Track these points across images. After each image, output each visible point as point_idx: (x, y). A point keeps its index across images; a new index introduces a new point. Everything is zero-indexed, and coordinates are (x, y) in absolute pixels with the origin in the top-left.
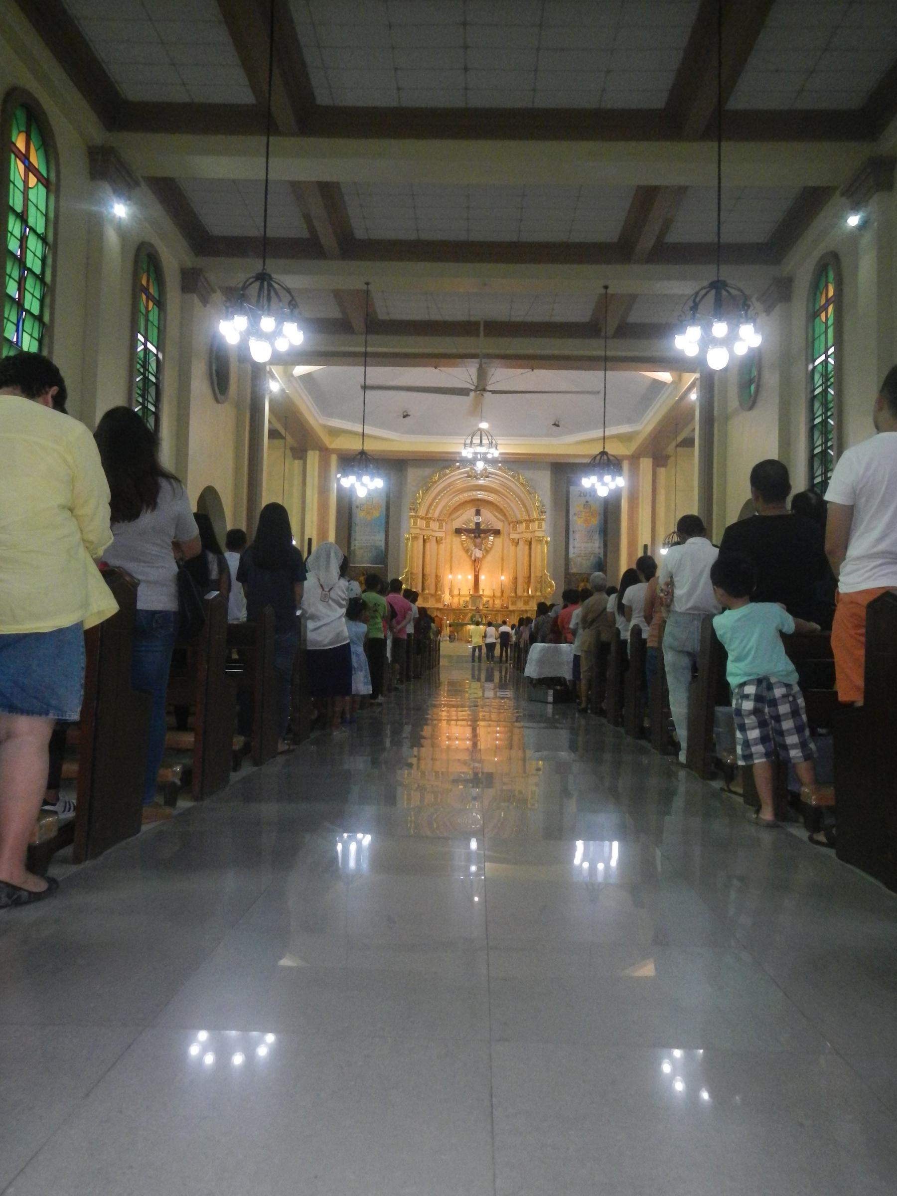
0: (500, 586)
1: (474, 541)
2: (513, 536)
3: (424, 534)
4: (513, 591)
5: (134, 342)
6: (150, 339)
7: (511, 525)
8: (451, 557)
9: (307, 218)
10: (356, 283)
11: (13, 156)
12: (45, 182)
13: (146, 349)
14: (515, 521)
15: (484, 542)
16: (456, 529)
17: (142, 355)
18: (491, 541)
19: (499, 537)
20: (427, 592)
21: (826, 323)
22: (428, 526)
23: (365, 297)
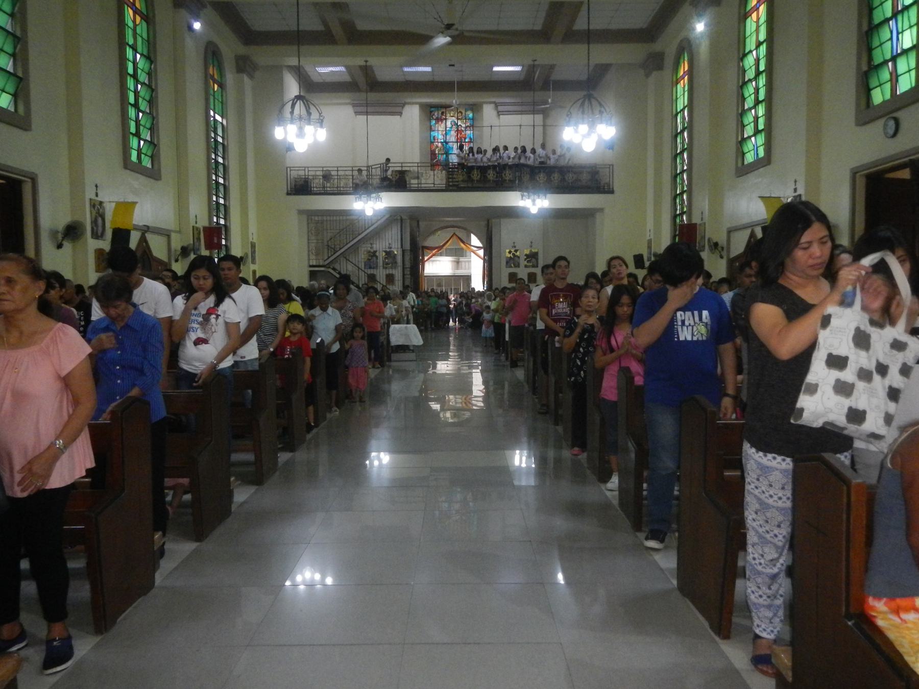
5: (207, 115)
6: (216, 111)
9: (324, 23)
10: (360, 62)
11: (126, 6)
12: (146, 18)
13: (215, 120)
17: (212, 123)
21: (684, 88)
23: (366, 70)
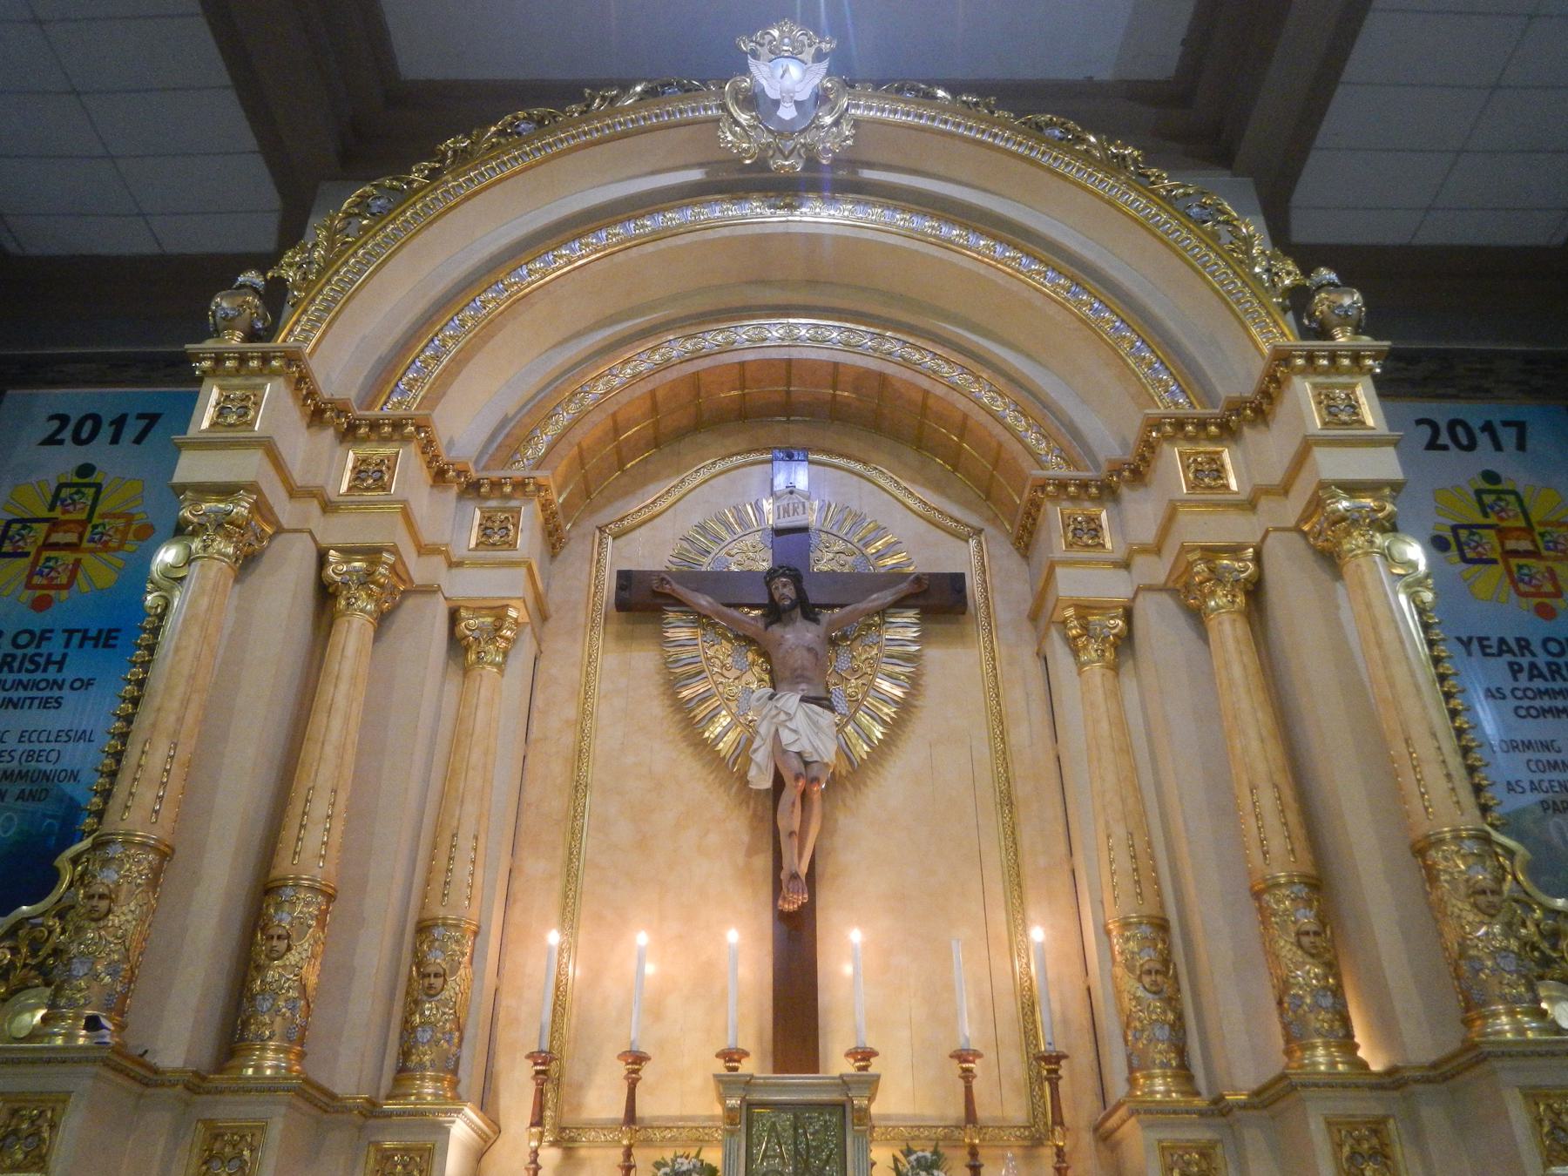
0: (1010, 1033)
1: (765, 654)
2: (1074, 583)
3: (325, 541)
4: (1161, 1052)
7: (1055, 514)
8: (578, 788)
14: (1084, 485)
15: (843, 662)
16: (626, 579)
18: (909, 658)
19: (962, 638)
20: (270, 1062)
22: (370, 476)
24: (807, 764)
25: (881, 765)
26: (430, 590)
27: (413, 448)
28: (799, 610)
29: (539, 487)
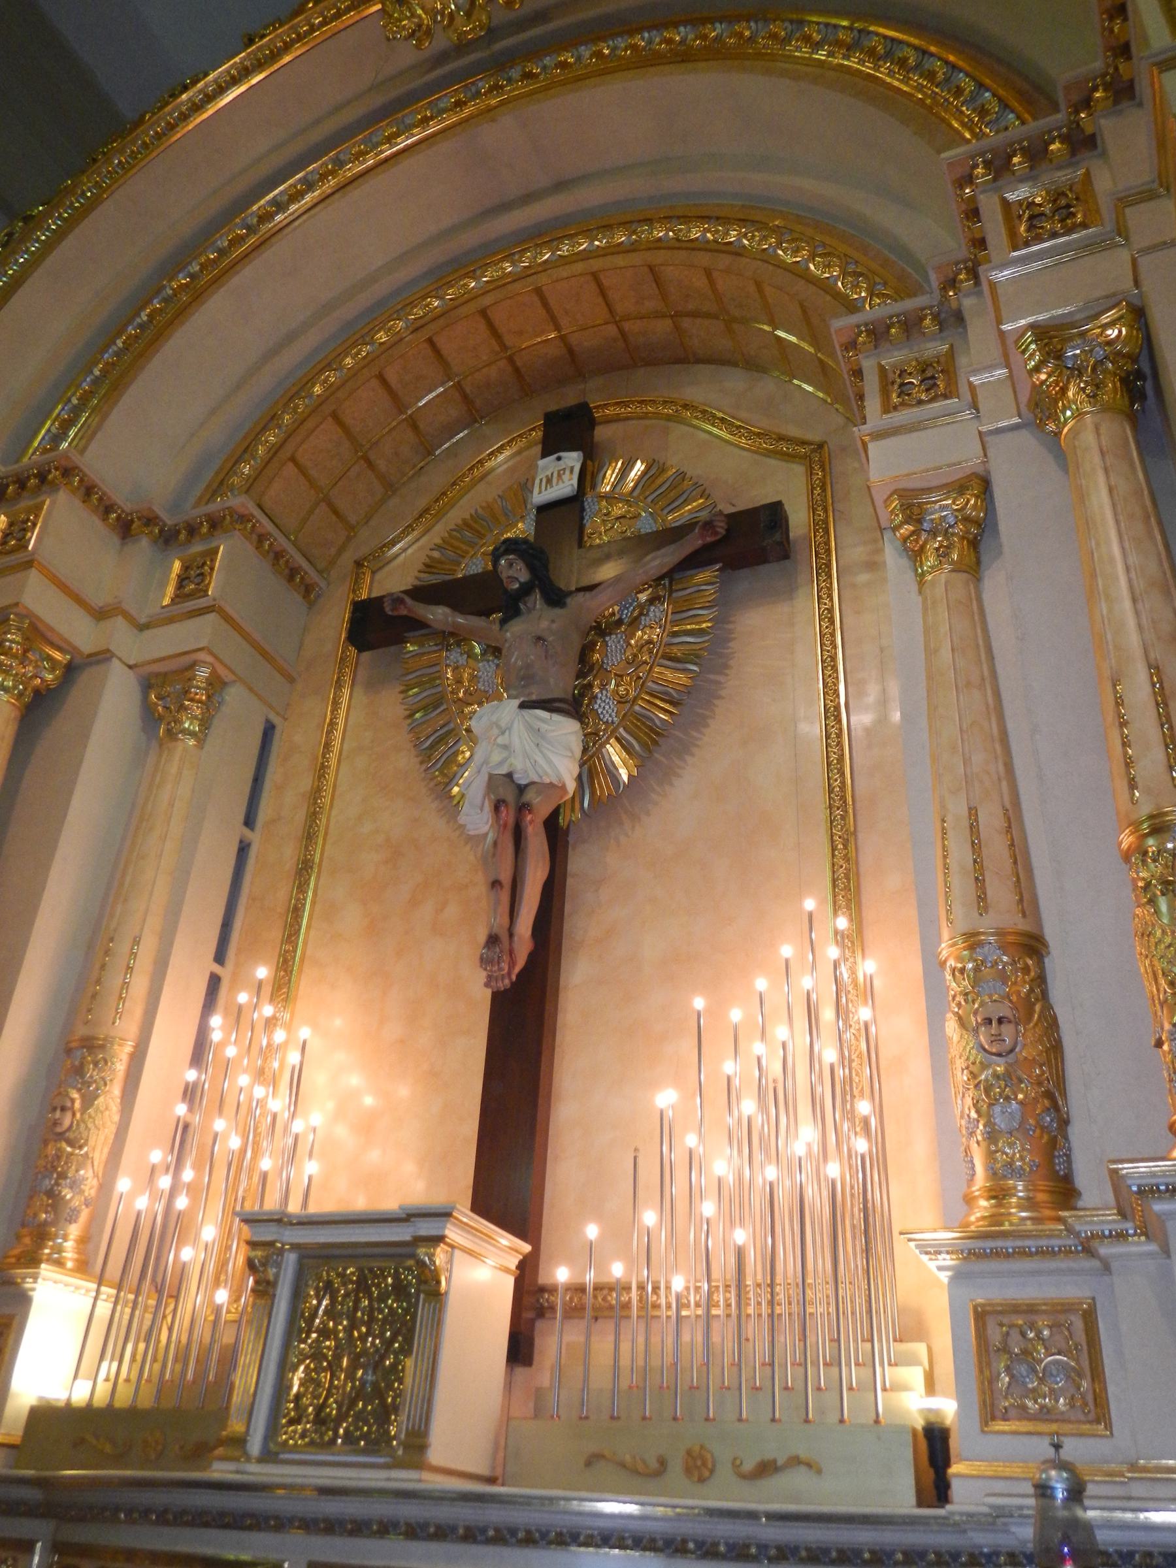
24: (521, 789)
25: (671, 785)
26: (102, 657)
27: (62, 496)
28: (537, 595)
29: (244, 518)
